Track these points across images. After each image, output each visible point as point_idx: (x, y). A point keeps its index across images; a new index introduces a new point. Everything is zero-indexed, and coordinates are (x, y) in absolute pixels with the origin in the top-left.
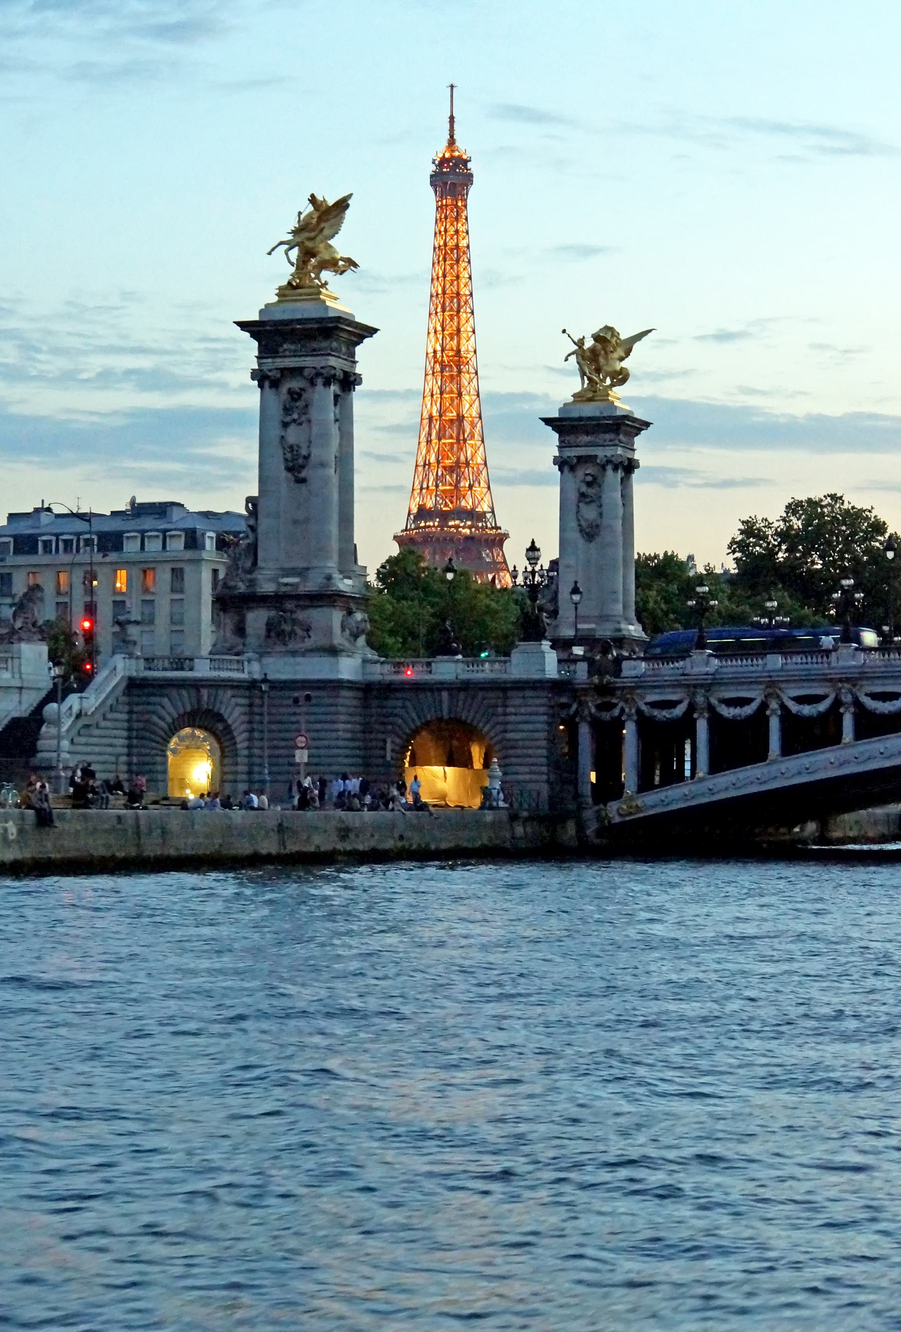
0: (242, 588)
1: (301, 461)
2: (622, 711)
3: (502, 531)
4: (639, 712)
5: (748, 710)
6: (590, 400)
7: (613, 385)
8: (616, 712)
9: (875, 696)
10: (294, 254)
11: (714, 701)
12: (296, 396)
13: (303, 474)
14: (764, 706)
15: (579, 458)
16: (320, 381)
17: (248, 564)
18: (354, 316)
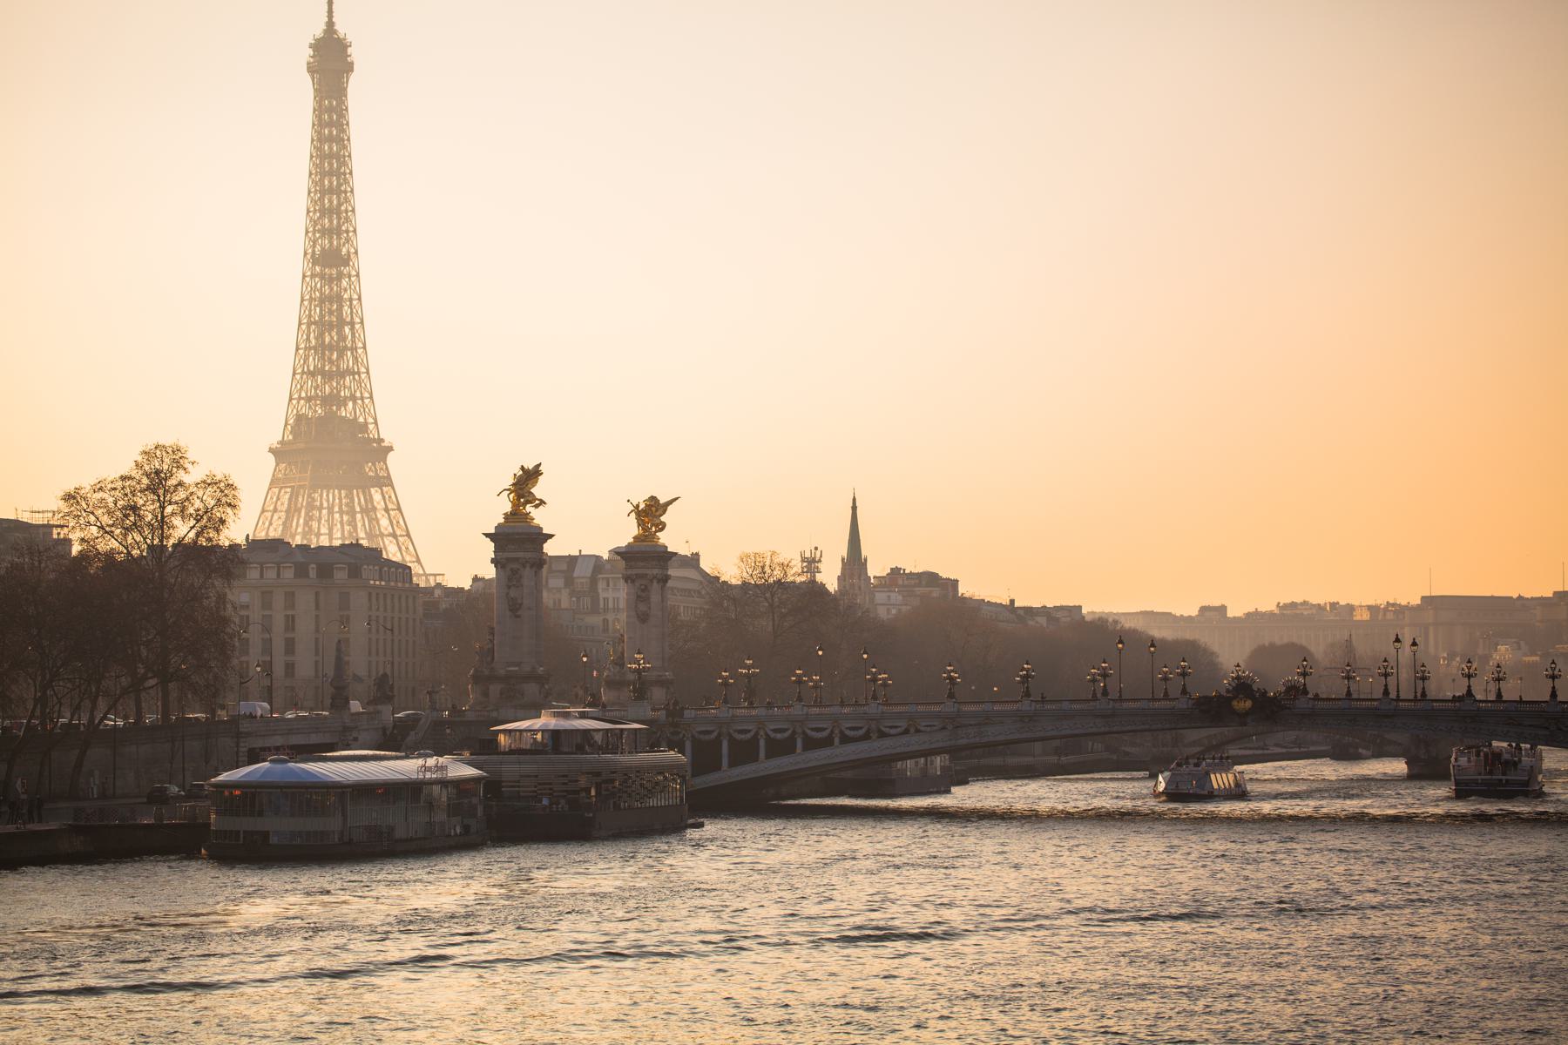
0: (487, 672)
1: (518, 606)
2: (684, 735)
3: (385, 444)
4: (693, 736)
5: (749, 736)
6: (643, 541)
7: (656, 532)
8: (681, 735)
9: (812, 729)
10: (512, 496)
11: (731, 731)
12: (514, 572)
13: (519, 613)
14: (757, 734)
15: (636, 575)
16: (528, 565)
17: (489, 659)
18: (541, 529)
